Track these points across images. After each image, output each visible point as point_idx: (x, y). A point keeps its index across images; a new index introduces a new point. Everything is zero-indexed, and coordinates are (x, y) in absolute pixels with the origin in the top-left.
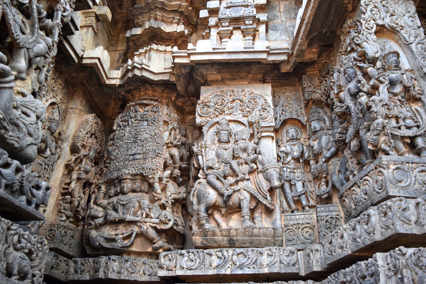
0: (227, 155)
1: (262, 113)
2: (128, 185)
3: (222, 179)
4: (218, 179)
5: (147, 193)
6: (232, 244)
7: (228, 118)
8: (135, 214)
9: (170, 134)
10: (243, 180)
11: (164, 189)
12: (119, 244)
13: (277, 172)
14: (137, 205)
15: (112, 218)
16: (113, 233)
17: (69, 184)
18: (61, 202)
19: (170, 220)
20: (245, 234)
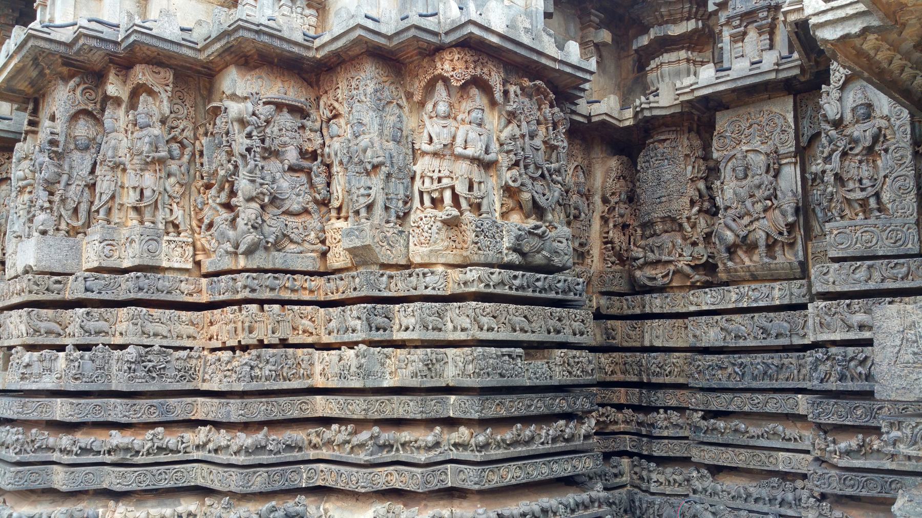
0: (743, 192)
1: (782, 136)
2: (659, 227)
3: (737, 219)
4: (734, 220)
5: (679, 231)
6: (754, 278)
7: (745, 148)
8: (669, 254)
9: (694, 167)
10: (758, 219)
11: (694, 226)
12: (660, 282)
13: (792, 208)
14: (671, 244)
15: (650, 260)
16: (654, 272)
17: (608, 232)
18: (604, 251)
19: (703, 256)
20: (763, 269)
